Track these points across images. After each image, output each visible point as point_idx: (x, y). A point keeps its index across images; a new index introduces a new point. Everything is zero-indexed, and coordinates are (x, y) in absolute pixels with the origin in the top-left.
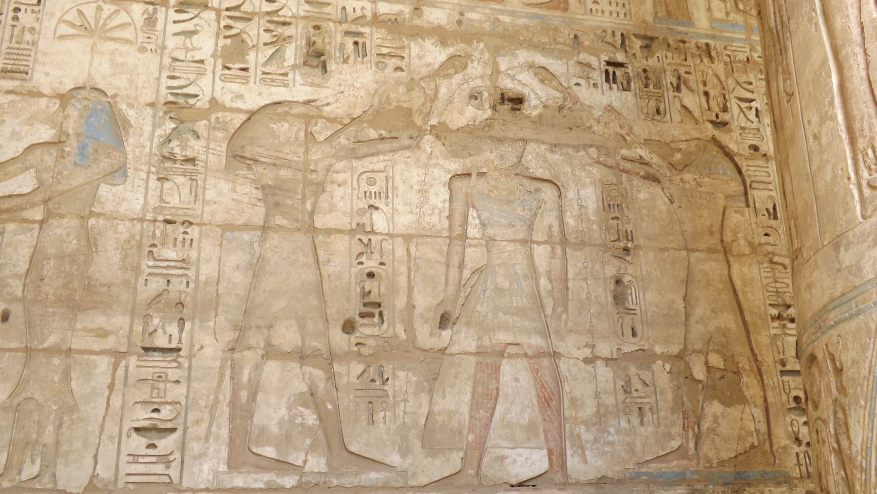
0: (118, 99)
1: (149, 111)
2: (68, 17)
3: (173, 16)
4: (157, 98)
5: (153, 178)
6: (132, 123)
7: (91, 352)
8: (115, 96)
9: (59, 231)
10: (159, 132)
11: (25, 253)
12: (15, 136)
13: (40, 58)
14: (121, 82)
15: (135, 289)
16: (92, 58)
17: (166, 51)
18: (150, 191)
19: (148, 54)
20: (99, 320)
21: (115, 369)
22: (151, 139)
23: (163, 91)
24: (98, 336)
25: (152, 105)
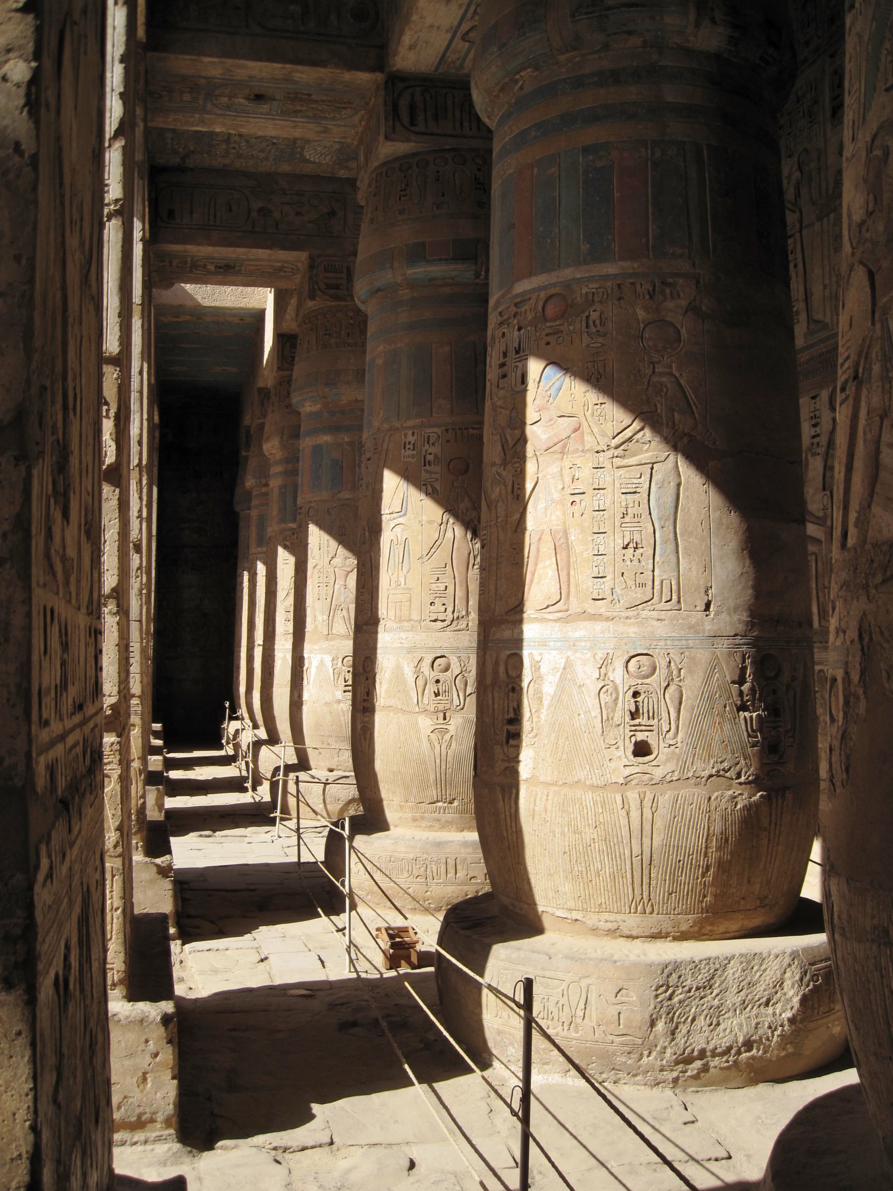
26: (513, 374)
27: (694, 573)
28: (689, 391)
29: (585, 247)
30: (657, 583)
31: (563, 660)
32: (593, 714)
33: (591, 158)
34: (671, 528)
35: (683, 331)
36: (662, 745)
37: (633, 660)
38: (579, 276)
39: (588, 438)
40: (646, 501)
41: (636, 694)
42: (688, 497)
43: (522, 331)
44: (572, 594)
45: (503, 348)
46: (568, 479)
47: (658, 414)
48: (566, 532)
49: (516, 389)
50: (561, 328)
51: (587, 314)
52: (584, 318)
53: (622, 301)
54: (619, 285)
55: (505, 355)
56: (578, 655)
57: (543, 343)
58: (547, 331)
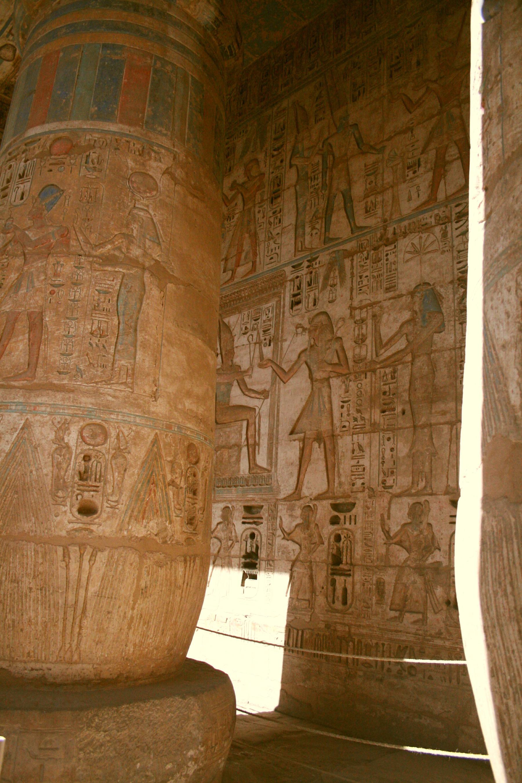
0: (436, 285)
1: (451, 286)
2: (408, 249)
3: (455, 225)
4: (454, 278)
5: (457, 322)
6: (444, 296)
7: (441, 424)
8: (434, 284)
9: (419, 364)
10: (457, 296)
11: (407, 378)
12: (395, 320)
13: (400, 276)
14: (436, 275)
15: (456, 386)
16: (421, 267)
17: (454, 248)
18: (457, 331)
19: (446, 253)
20: (442, 406)
21: (451, 432)
22: (454, 302)
23: (456, 272)
24: (442, 415)
25: (452, 282)
26: (14, 193)
27: (147, 364)
28: (159, 226)
29: (94, 109)
30: (116, 366)
31: (23, 422)
32: (45, 471)
33: (109, 52)
34: (133, 324)
35: (160, 185)
36: (105, 504)
37: (87, 428)
38: (85, 127)
39: (73, 243)
40: (115, 299)
41: (87, 458)
42: (148, 304)
43: (29, 162)
44: (39, 365)
45: (8, 176)
46: (50, 272)
47: (134, 237)
48: (41, 315)
49: (15, 204)
50: (64, 160)
51: (88, 153)
52: (84, 156)
53: (117, 151)
54: (116, 140)
55: (8, 181)
56: (38, 418)
57: (47, 169)
58: (51, 161)
